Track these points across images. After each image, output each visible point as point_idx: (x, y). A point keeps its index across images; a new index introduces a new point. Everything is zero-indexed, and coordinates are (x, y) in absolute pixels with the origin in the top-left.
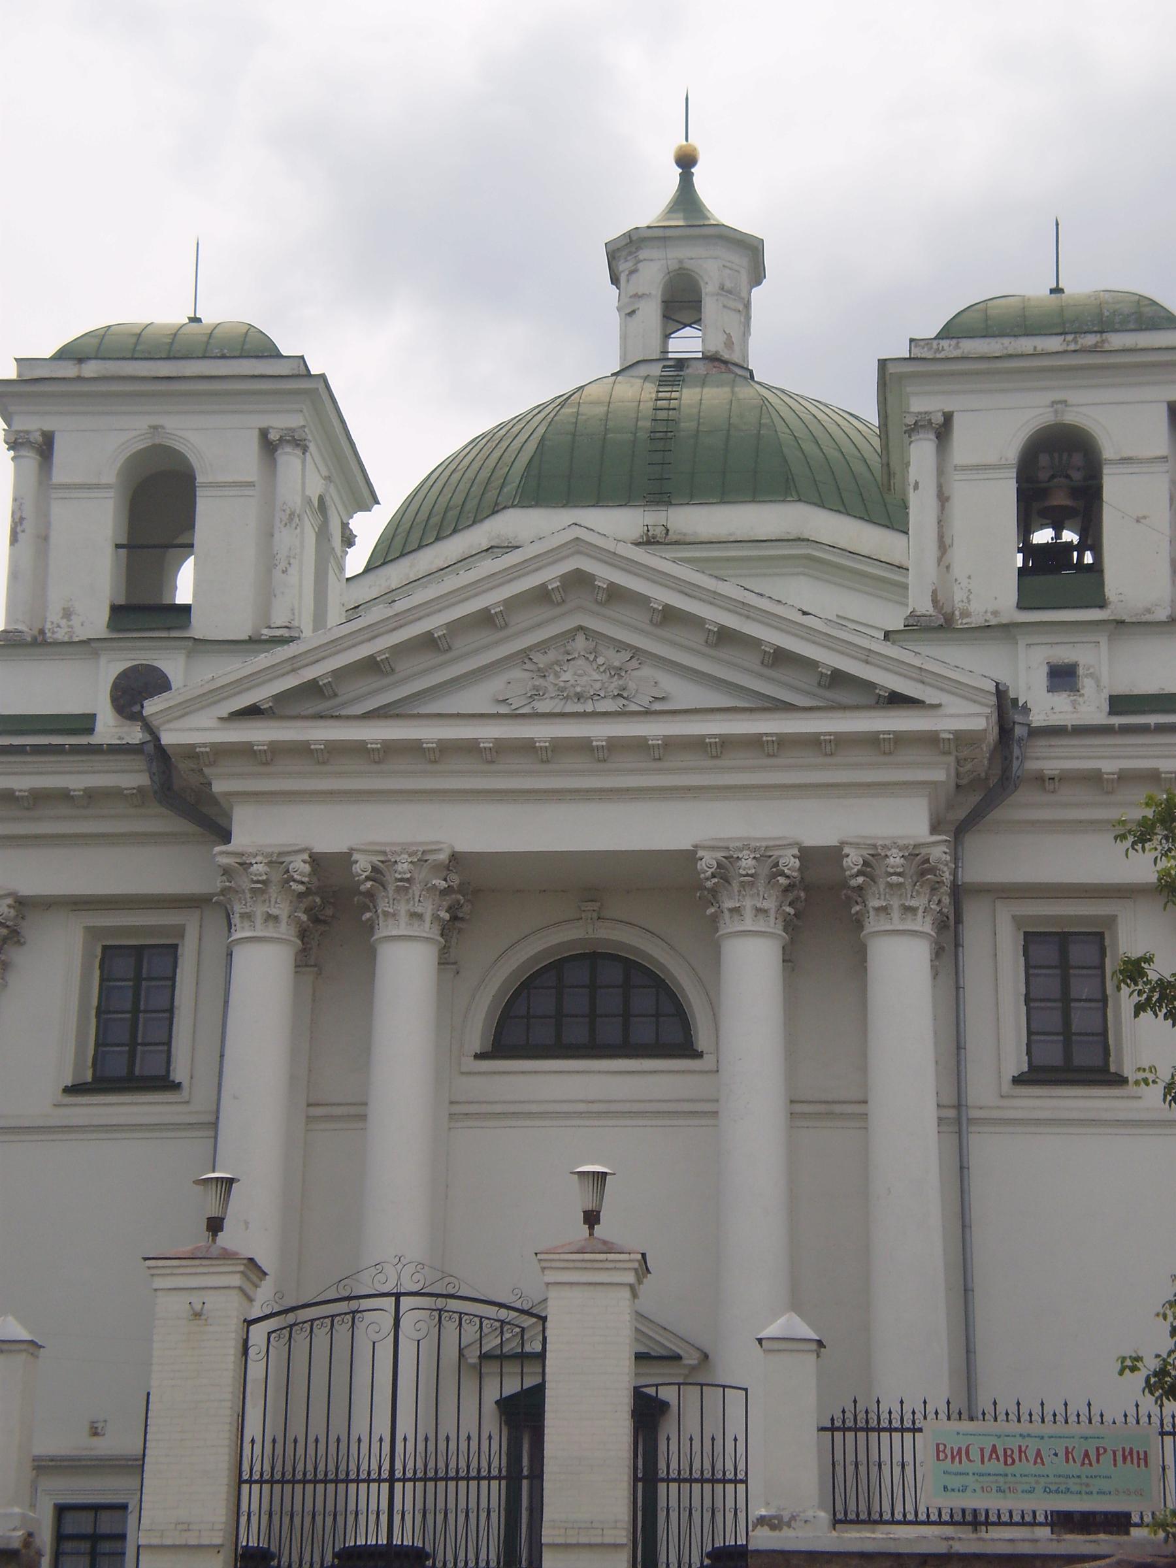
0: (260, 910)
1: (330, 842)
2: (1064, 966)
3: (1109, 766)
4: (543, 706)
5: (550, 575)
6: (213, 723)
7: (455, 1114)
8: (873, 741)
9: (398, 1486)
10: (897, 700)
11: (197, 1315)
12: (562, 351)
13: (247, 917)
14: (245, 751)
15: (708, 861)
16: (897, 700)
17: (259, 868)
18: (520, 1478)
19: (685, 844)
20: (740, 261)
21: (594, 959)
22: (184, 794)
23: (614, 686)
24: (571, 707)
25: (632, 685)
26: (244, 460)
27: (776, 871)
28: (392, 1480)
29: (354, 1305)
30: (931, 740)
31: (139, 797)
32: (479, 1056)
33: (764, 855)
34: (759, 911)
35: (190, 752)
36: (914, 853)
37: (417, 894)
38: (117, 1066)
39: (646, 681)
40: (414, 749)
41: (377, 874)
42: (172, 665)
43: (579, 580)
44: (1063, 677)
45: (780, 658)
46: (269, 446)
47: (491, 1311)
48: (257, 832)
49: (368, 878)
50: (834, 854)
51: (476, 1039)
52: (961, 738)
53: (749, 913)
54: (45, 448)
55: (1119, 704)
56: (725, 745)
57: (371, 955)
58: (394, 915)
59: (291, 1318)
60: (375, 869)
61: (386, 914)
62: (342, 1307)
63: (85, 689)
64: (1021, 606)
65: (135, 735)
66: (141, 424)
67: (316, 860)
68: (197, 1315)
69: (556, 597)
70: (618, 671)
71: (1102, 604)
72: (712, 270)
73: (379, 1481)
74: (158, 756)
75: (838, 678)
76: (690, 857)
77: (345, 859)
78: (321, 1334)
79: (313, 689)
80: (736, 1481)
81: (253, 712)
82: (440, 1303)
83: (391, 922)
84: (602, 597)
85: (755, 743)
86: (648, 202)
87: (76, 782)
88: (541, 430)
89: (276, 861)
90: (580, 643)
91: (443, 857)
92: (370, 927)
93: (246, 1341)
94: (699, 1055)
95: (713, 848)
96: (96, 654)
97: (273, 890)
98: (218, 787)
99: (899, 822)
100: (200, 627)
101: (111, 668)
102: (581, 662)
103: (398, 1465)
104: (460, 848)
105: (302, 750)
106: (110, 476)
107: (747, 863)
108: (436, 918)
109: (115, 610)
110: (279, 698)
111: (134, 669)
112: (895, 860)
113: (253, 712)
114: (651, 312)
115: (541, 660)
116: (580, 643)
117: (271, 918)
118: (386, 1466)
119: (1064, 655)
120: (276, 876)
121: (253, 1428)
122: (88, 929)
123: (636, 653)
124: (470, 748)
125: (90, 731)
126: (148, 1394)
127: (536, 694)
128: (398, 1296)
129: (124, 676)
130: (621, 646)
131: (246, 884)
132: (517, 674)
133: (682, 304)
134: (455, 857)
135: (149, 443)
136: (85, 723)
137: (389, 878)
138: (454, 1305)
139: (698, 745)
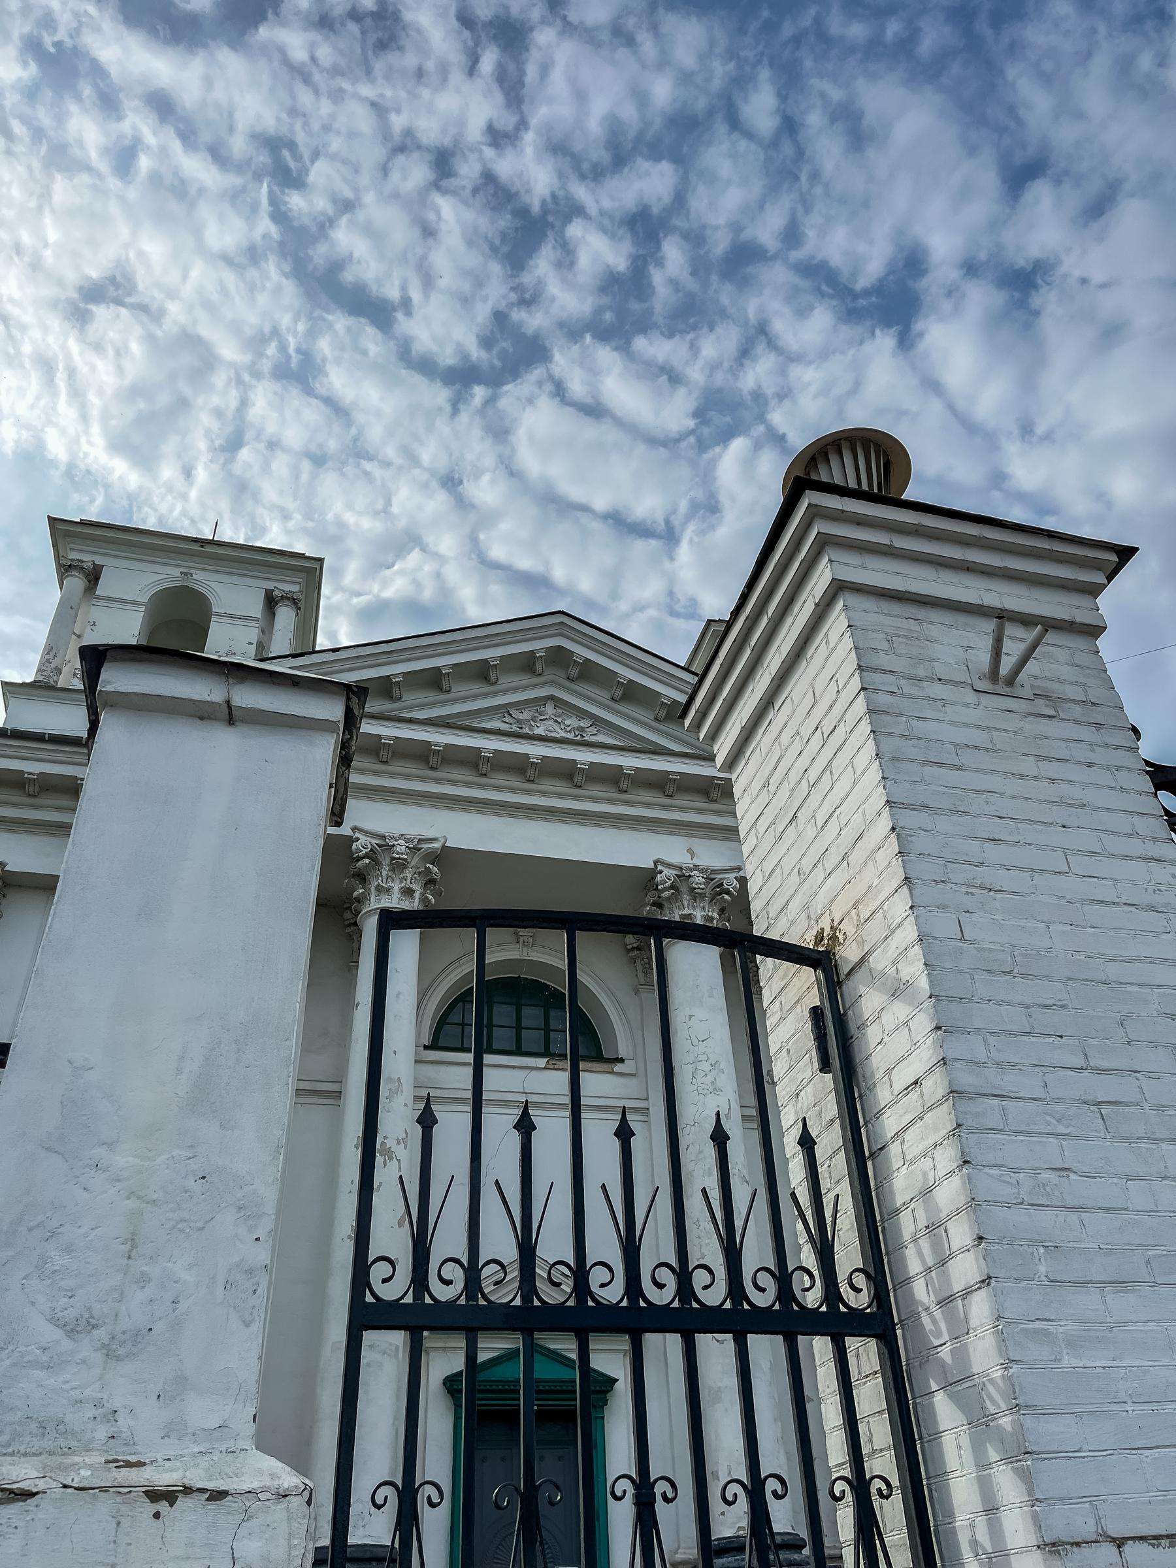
5: (538, 646)
32: (426, 1047)
37: (409, 876)
41: (372, 855)
43: (558, 657)
46: (271, 602)
49: (366, 856)
54: (93, 576)
58: (388, 890)
61: (379, 889)
66: (176, 572)
69: (539, 667)
83: (384, 897)
84: (574, 672)
90: (550, 709)
91: (437, 845)
94: (622, 1060)
102: (551, 722)
106: (145, 599)
107: (698, 879)
130: (583, 714)
135: (179, 584)
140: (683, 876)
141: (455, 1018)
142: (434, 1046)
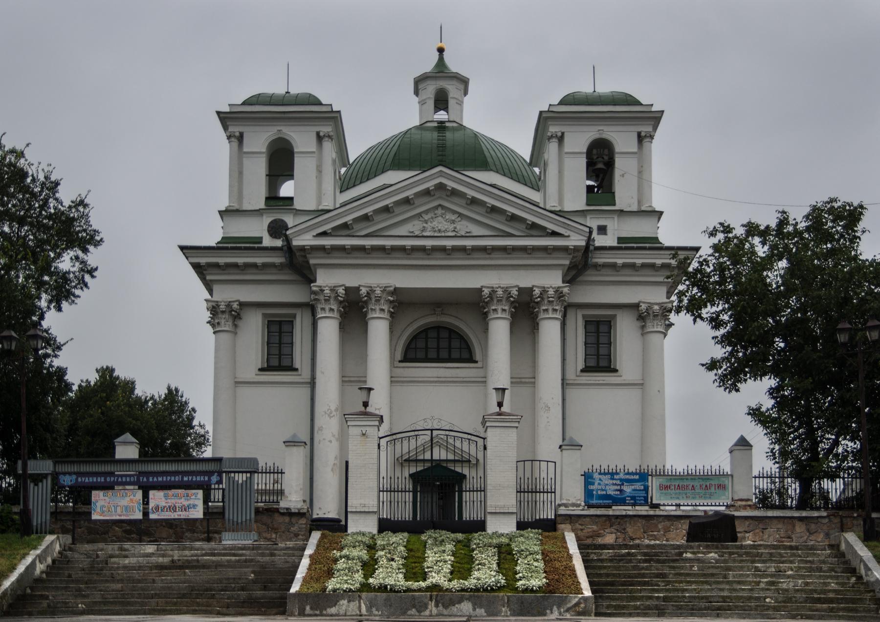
0: (327, 307)
1: (352, 283)
2: (598, 332)
3: (620, 261)
4: (425, 234)
6: (311, 237)
7: (394, 381)
8: (545, 249)
10: (554, 234)
11: (364, 435)
12: (405, 114)
13: (323, 309)
14: (322, 249)
15: (486, 291)
16: (554, 234)
17: (327, 291)
19: (478, 286)
20: (462, 87)
21: (438, 328)
22: (298, 265)
23: (452, 227)
24: (436, 234)
25: (458, 227)
26: (312, 146)
27: (509, 295)
29: (416, 433)
30: (565, 249)
31: (280, 267)
32: (400, 362)
33: (506, 290)
34: (504, 310)
35: (302, 249)
36: (557, 290)
38: (275, 362)
39: (464, 227)
40: (382, 249)
42: (290, 220)
44: (602, 230)
45: (514, 218)
47: (466, 436)
48: (325, 279)
50: (530, 290)
51: (399, 356)
52: (576, 249)
53: (500, 311)
55: (620, 240)
56: (495, 249)
57: (366, 324)
59: (394, 437)
60: (368, 293)
61: (372, 309)
63: (257, 228)
64: (588, 205)
65: (279, 243)
67: (347, 289)
68: (364, 435)
70: (453, 222)
71: (614, 205)
72: (453, 90)
74: (288, 249)
75: (534, 226)
76: (480, 290)
77: (358, 289)
78: (405, 443)
79: (345, 226)
81: (324, 234)
82: (447, 433)
85: (504, 249)
86: (428, 64)
87: (259, 260)
88: (398, 143)
89: (333, 289)
91: (392, 289)
92: (365, 315)
93: (379, 445)
95: (488, 287)
96: (262, 215)
97: (332, 301)
98: (312, 262)
99: (552, 280)
100: (297, 205)
101: (267, 220)
104: (397, 286)
105: (342, 249)
107: (500, 292)
108: (389, 311)
109: (267, 199)
110: (334, 229)
111: (275, 220)
112: (551, 292)
113: (324, 234)
114: (431, 104)
115: (426, 217)
116: (439, 211)
117: (331, 310)
119: (602, 222)
120: (333, 296)
121: (383, 473)
122: (263, 314)
123: (460, 215)
124: (403, 249)
125: (261, 242)
126: (347, 463)
127: (424, 229)
128: (432, 430)
129: (272, 222)
131: (322, 298)
132: (416, 222)
133: (441, 102)
134: (395, 289)
136: (259, 240)
137: (373, 296)
139: (484, 249)
140: (493, 291)
141: (413, 346)
142: (406, 359)
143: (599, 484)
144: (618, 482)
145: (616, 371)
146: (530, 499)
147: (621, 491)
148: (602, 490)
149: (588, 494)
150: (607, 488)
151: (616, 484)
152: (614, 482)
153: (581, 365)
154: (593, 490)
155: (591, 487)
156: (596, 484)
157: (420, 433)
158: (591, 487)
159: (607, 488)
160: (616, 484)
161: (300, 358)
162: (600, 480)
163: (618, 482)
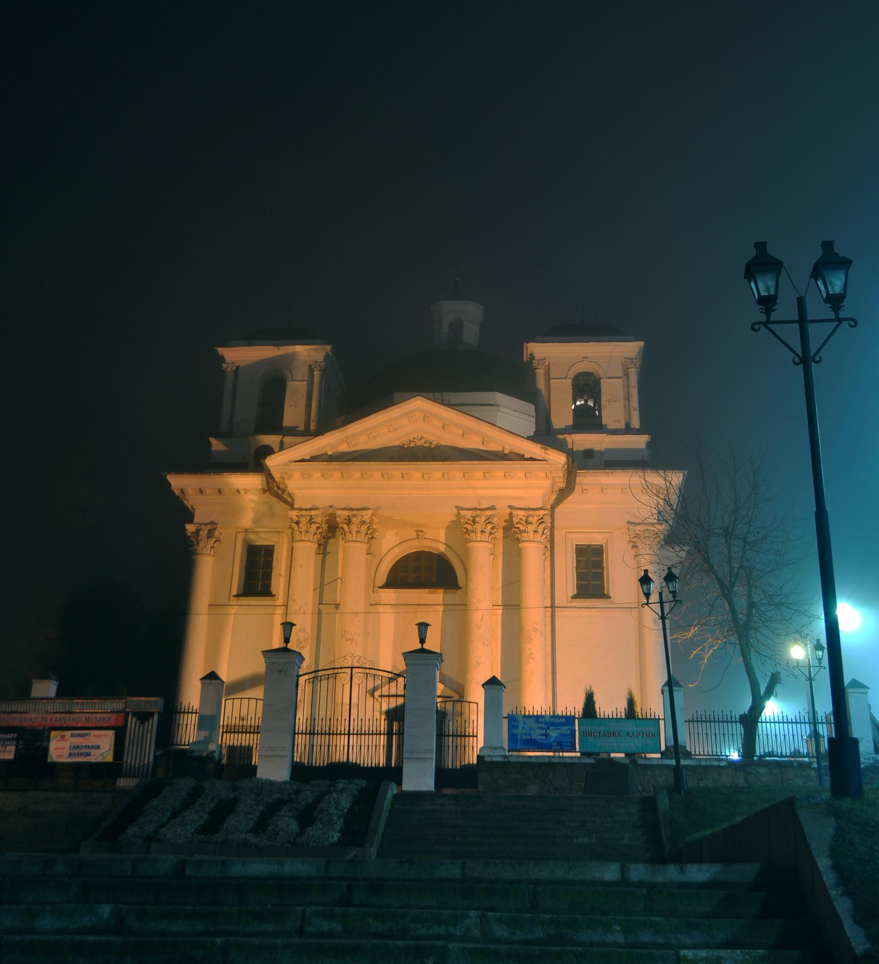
9: (351, 736)
18: (393, 734)
28: (349, 734)
29: (336, 671)
47: (386, 674)
62: (331, 672)
73: (344, 734)
80: (473, 736)
82: (367, 671)
103: (351, 729)
118: (347, 729)
128: (352, 668)
138: (372, 672)
143: (523, 728)
144: (544, 726)
145: (608, 597)
146: (450, 744)
147: (546, 735)
148: (527, 734)
149: (512, 738)
150: (532, 732)
151: (541, 728)
152: (539, 725)
153: (572, 590)
154: (517, 735)
155: (516, 731)
156: (520, 727)
157: (340, 671)
158: (516, 731)
159: (532, 732)
160: (541, 728)
161: (278, 584)
162: (524, 723)
163: (544, 726)
